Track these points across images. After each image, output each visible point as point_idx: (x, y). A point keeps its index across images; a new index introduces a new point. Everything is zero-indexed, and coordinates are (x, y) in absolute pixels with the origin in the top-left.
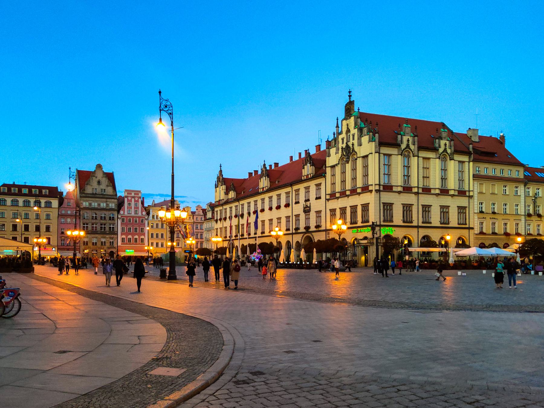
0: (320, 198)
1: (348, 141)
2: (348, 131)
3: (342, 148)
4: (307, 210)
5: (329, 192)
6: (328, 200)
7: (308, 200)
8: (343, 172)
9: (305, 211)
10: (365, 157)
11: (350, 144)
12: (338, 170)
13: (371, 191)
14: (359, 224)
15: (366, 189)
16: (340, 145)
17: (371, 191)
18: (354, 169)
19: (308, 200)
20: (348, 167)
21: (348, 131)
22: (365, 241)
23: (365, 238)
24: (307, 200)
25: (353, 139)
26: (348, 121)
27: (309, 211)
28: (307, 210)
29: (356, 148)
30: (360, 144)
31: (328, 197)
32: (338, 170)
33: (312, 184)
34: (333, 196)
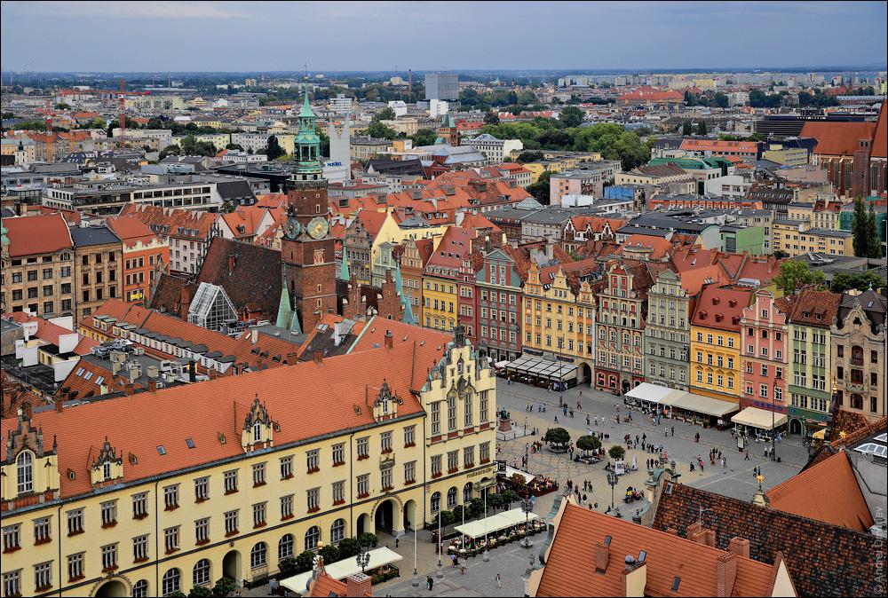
0: (413, 445)
1: (461, 372)
2: (461, 360)
3: (453, 381)
4: (386, 467)
5: (429, 435)
6: (428, 446)
7: (390, 451)
8: (452, 412)
9: (382, 467)
10: (484, 393)
11: (466, 378)
12: (444, 407)
13: (493, 429)
14: (477, 465)
15: (485, 427)
16: (449, 378)
17: (493, 429)
18: (468, 407)
19: (390, 451)
20: (460, 404)
21: (461, 360)
22: (488, 483)
23: (485, 480)
24: (387, 450)
25: (469, 371)
26: (460, 350)
27: (392, 463)
28: (386, 467)
29: (473, 382)
30: (478, 377)
31: (429, 442)
32: (444, 407)
33: (398, 432)
34: (436, 439)
